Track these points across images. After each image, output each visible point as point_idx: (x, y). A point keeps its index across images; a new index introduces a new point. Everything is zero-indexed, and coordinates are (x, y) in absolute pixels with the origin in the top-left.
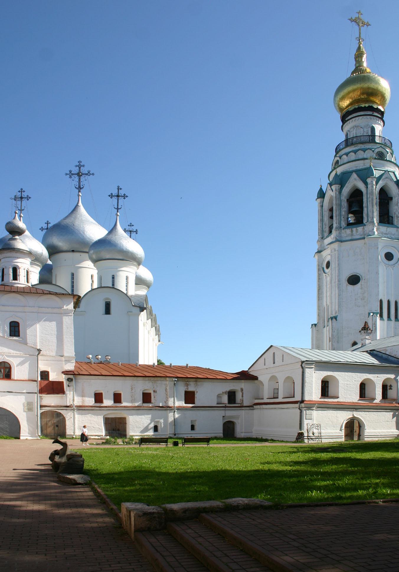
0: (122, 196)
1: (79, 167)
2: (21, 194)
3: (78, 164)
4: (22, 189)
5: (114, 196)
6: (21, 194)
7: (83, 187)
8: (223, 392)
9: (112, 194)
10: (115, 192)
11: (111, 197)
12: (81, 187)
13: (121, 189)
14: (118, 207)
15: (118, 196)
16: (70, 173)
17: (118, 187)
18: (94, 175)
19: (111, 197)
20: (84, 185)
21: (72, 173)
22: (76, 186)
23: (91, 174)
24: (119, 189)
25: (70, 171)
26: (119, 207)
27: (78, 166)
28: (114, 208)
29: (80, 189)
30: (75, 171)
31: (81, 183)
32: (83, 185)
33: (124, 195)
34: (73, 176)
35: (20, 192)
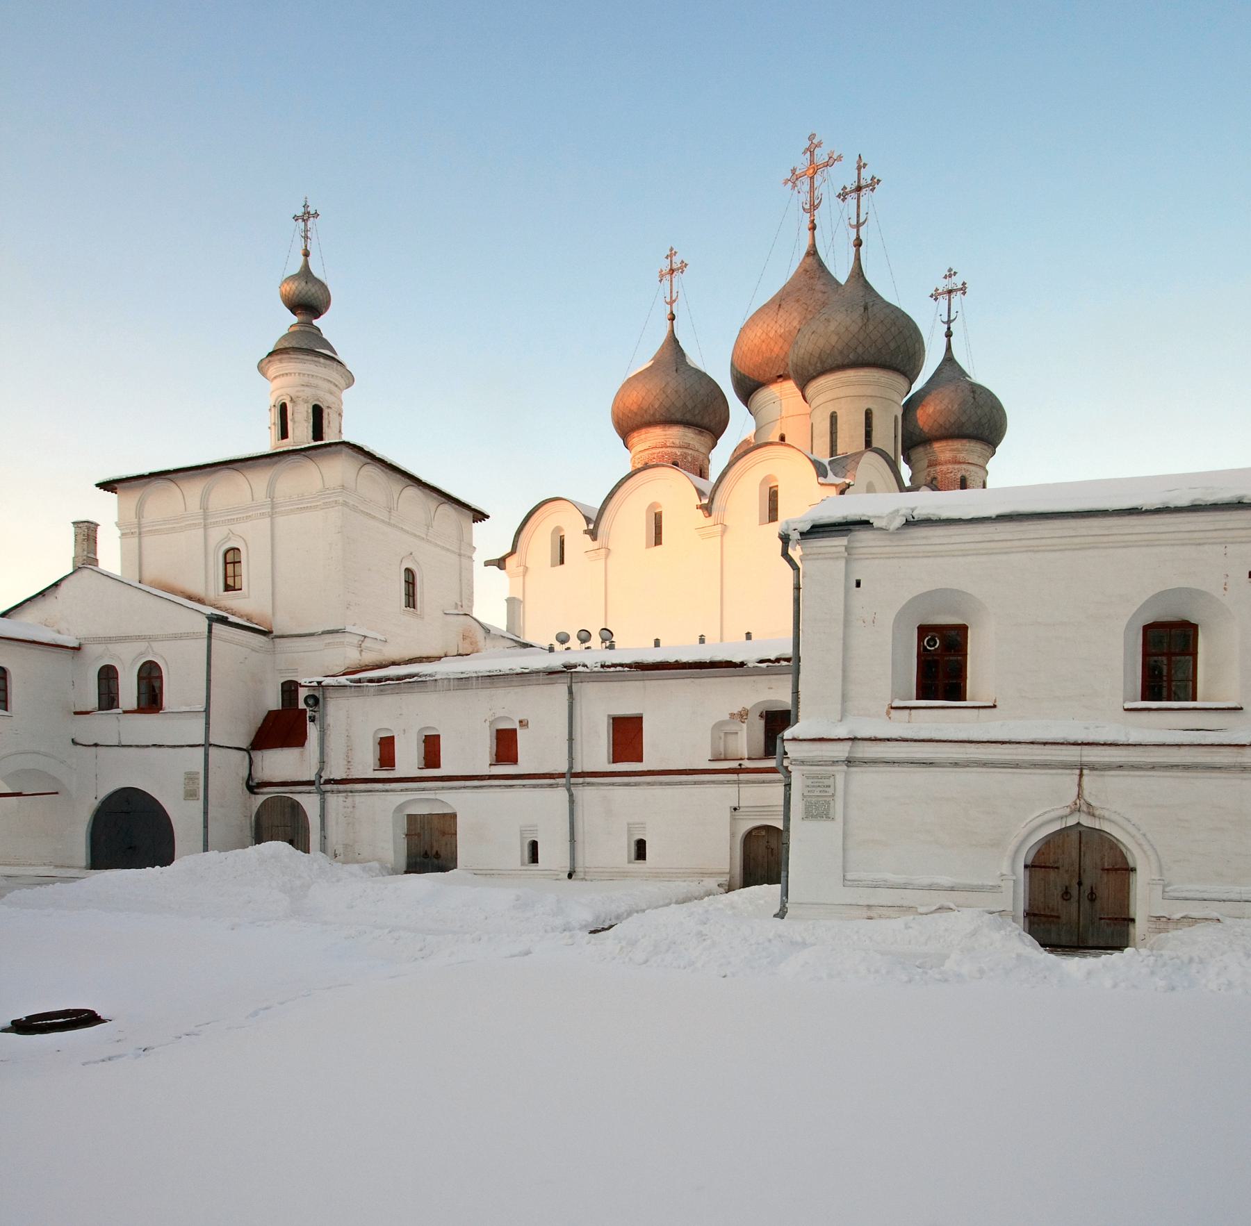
1: (810, 152)
3: (807, 144)
5: (851, 192)
7: (820, 202)
8: (732, 715)
9: (845, 188)
11: (842, 197)
14: (858, 221)
15: (859, 189)
18: (841, 160)
20: (822, 194)
23: (835, 160)
25: (794, 171)
26: (861, 220)
27: (808, 149)
28: (850, 225)
30: (802, 167)
33: (873, 178)
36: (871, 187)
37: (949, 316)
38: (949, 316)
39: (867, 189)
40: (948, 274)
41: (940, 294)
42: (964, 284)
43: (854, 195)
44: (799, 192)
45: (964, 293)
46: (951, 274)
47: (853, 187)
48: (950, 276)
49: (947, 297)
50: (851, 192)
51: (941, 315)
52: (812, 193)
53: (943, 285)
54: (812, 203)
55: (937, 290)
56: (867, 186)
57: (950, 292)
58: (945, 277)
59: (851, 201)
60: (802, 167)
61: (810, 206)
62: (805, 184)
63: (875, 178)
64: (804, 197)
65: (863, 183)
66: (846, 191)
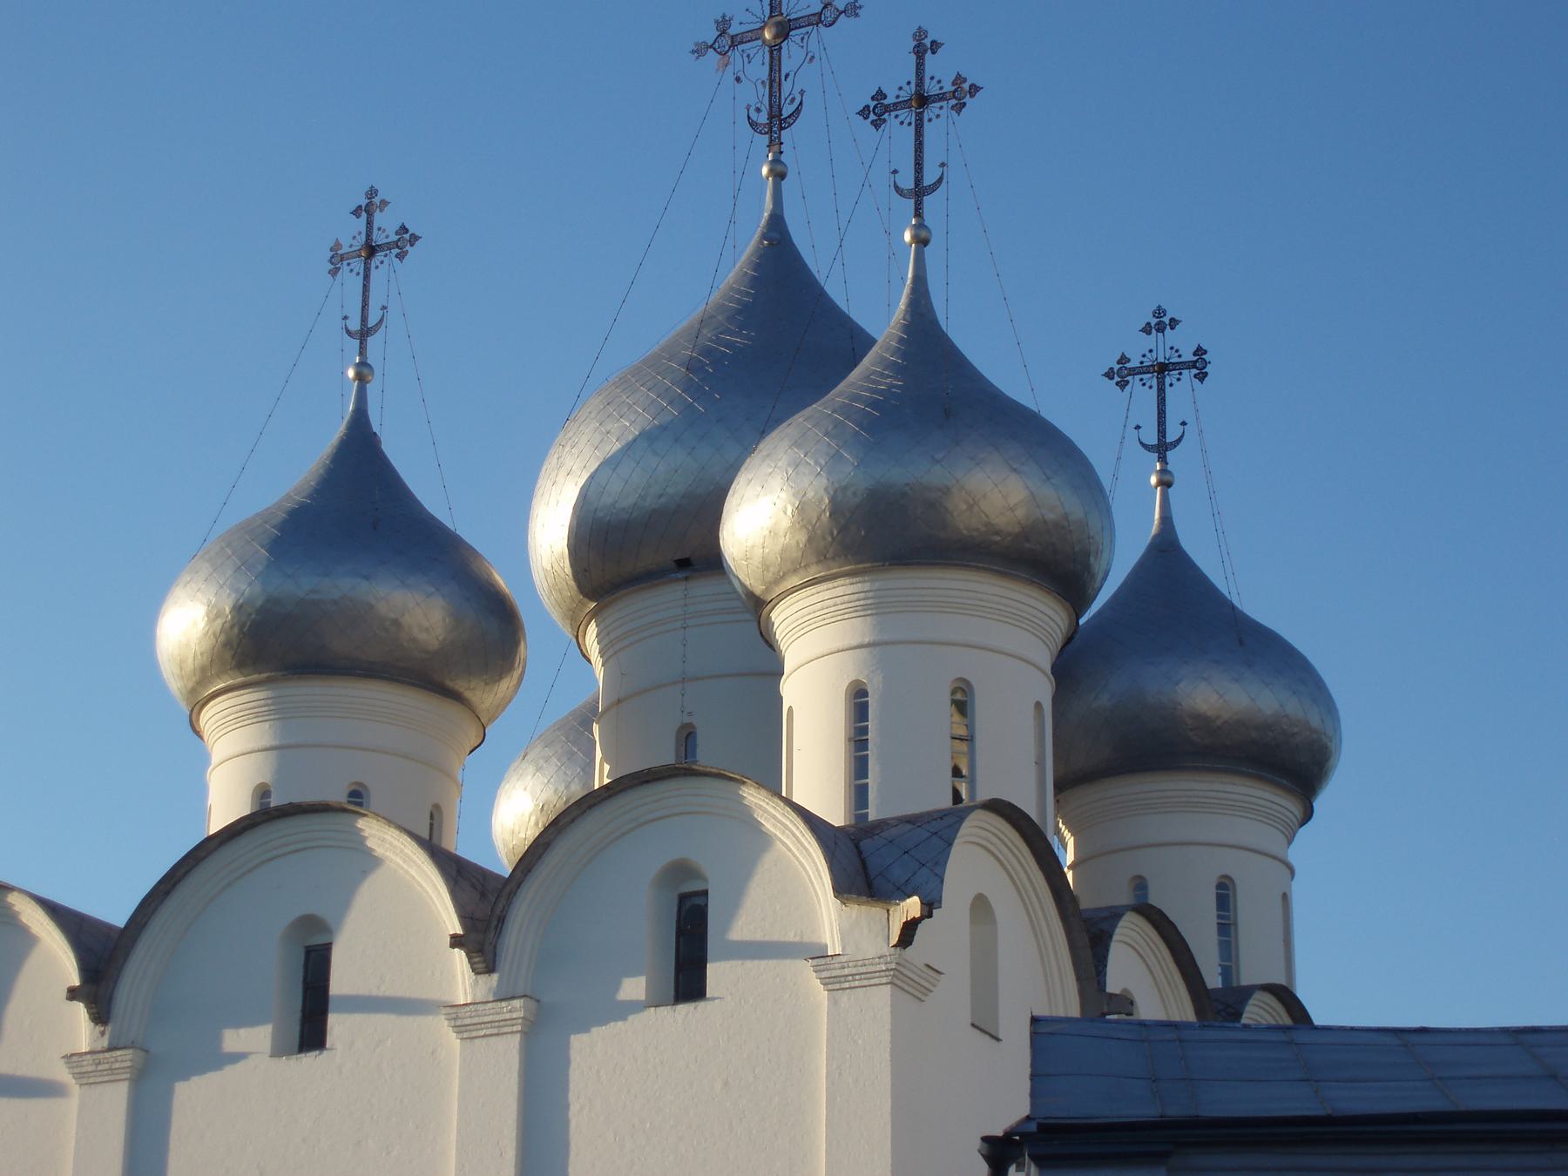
0: (941, 97)
2: (369, 223)
4: (372, 193)
5: (896, 106)
6: (369, 223)
7: (798, 111)
9: (880, 95)
10: (897, 80)
11: (872, 117)
12: (786, 112)
13: (935, 46)
14: (918, 180)
15: (922, 100)
16: (723, 33)
17: (920, 34)
18: (857, 15)
19: (872, 117)
20: (802, 93)
21: (732, 31)
22: (754, 116)
24: (923, 48)
26: (929, 179)
28: (897, 188)
29: (782, 129)
30: (748, 17)
31: (786, 87)
32: (793, 100)
33: (959, 80)
34: (735, 55)
35: (364, 215)
36: (954, 102)
37: (1162, 432)
38: (1162, 432)
39: (944, 104)
40: (1154, 321)
41: (1134, 372)
42: (1200, 351)
43: (906, 115)
44: (738, 80)
45: (1202, 377)
46: (1161, 323)
47: (904, 96)
48: (1161, 328)
49: (1154, 382)
50: (896, 106)
51: (1138, 427)
52: (775, 85)
53: (1139, 348)
54: (775, 109)
55: (1123, 360)
56: (941, 97)
57: (1162, 369)
58: (1147, 330)
59: (899, 131)
60: (748, 17)
61: (771, 117)
62: (757, 60)
63: (965, 80)
64: (754, 94)
65: (931, 88)
66: (886, 102)
